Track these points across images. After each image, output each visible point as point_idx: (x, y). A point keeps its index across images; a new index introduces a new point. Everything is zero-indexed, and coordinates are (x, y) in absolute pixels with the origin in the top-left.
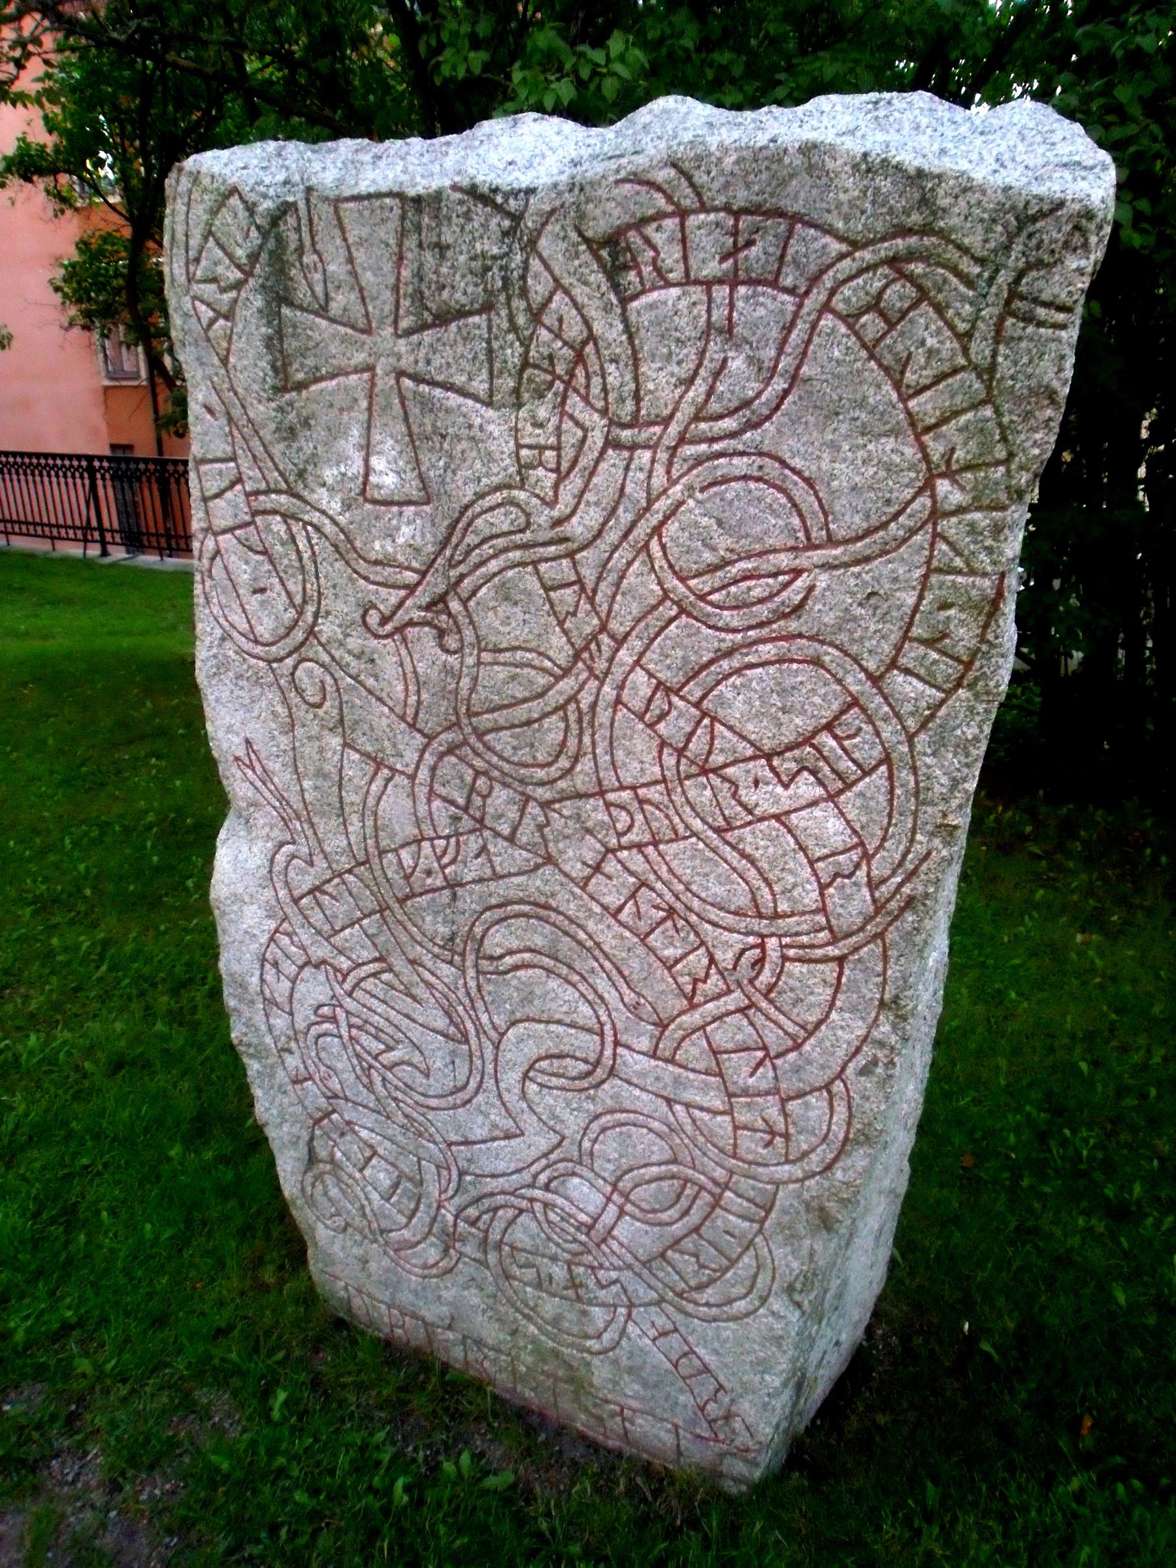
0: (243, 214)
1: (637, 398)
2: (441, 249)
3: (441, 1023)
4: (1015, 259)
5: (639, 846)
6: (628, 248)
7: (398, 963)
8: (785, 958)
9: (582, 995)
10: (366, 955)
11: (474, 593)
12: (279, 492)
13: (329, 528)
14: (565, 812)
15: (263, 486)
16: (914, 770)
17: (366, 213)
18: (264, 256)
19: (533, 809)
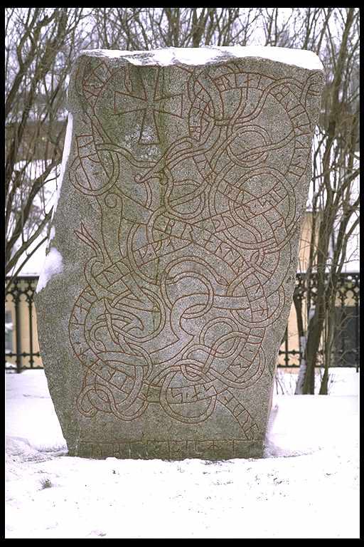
7: (136, 290)
8: (264, 253)
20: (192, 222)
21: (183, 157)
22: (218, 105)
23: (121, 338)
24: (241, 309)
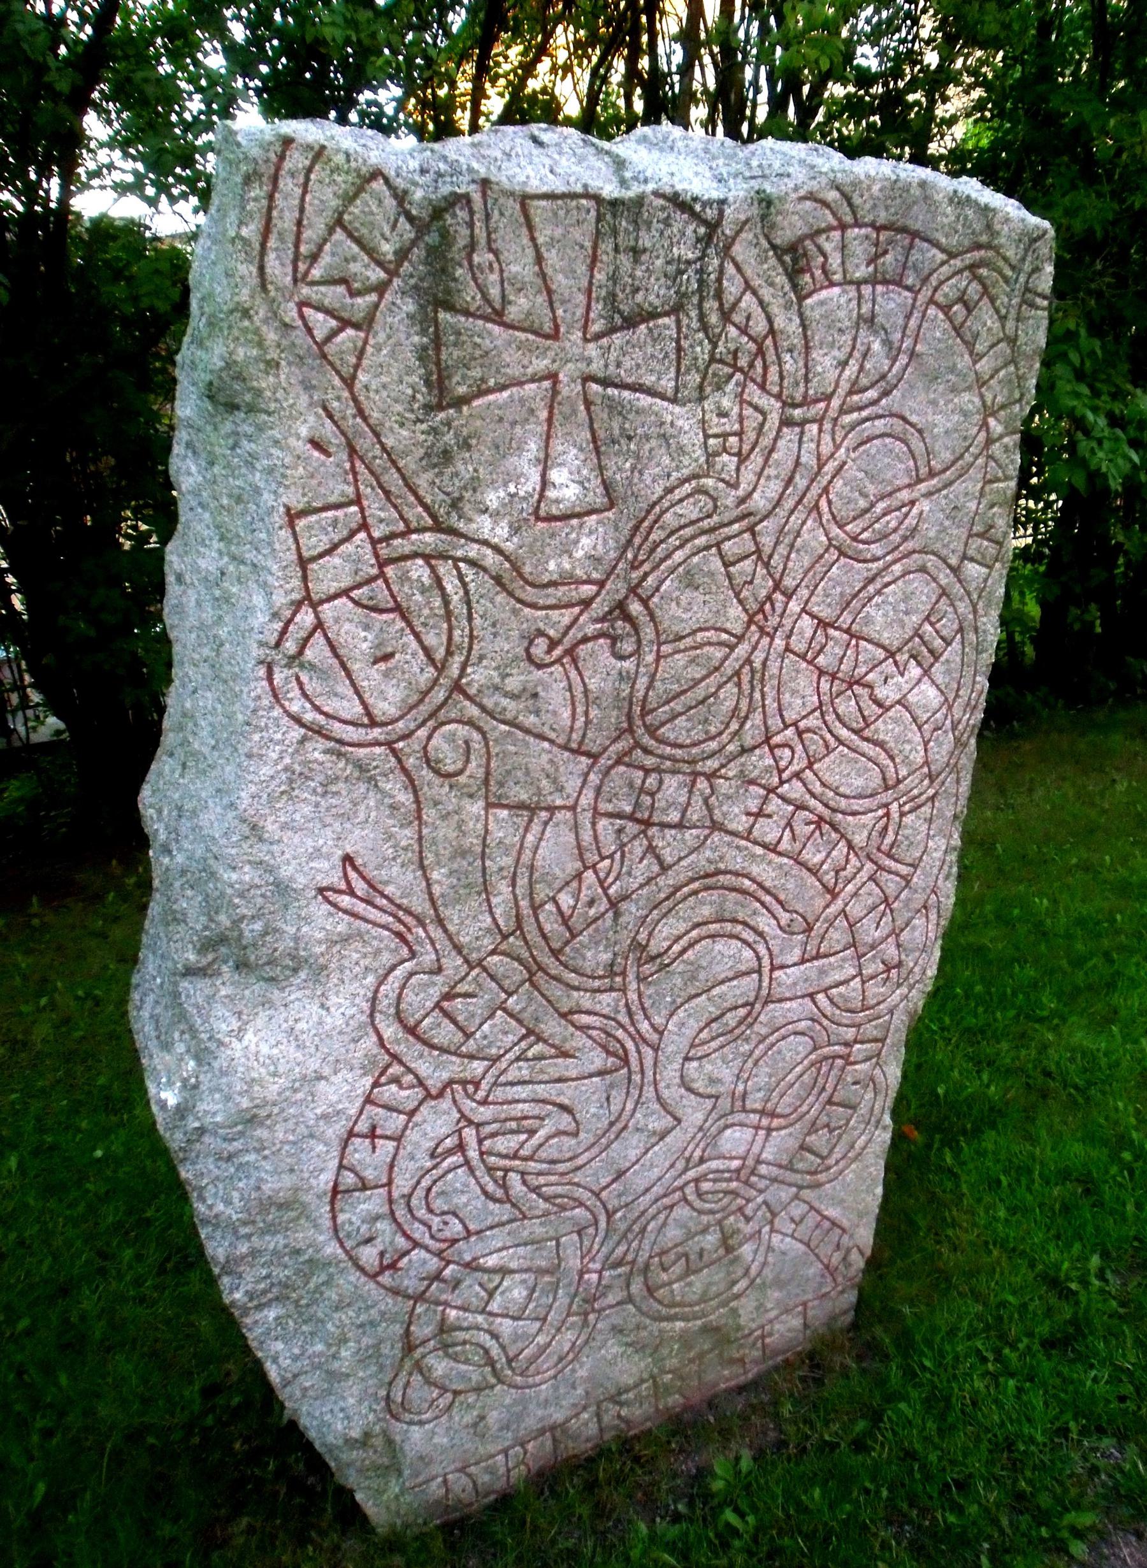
0: (390, 202)
1: (807, 380)
2: (636, 252)
3: (597, 1059)
4: (1027, 267)
5: (797, 775)
6: (805, 255)
7: (552, 1027)
8: (902, 814)
9: (744, 942)
10: (511, 1038)
11: (657, 589)
12: (425, 530)
13: (490, 558)
14: (731, 774)
15: (401, 526)
16: (976, 630)
17: (562, 213)
18: (417, 253)
19: (702, 784)
20: (712, 764)
21: (688, 548)
22: (790, 351)
23: (514, 1178)
24: (837, 985)
